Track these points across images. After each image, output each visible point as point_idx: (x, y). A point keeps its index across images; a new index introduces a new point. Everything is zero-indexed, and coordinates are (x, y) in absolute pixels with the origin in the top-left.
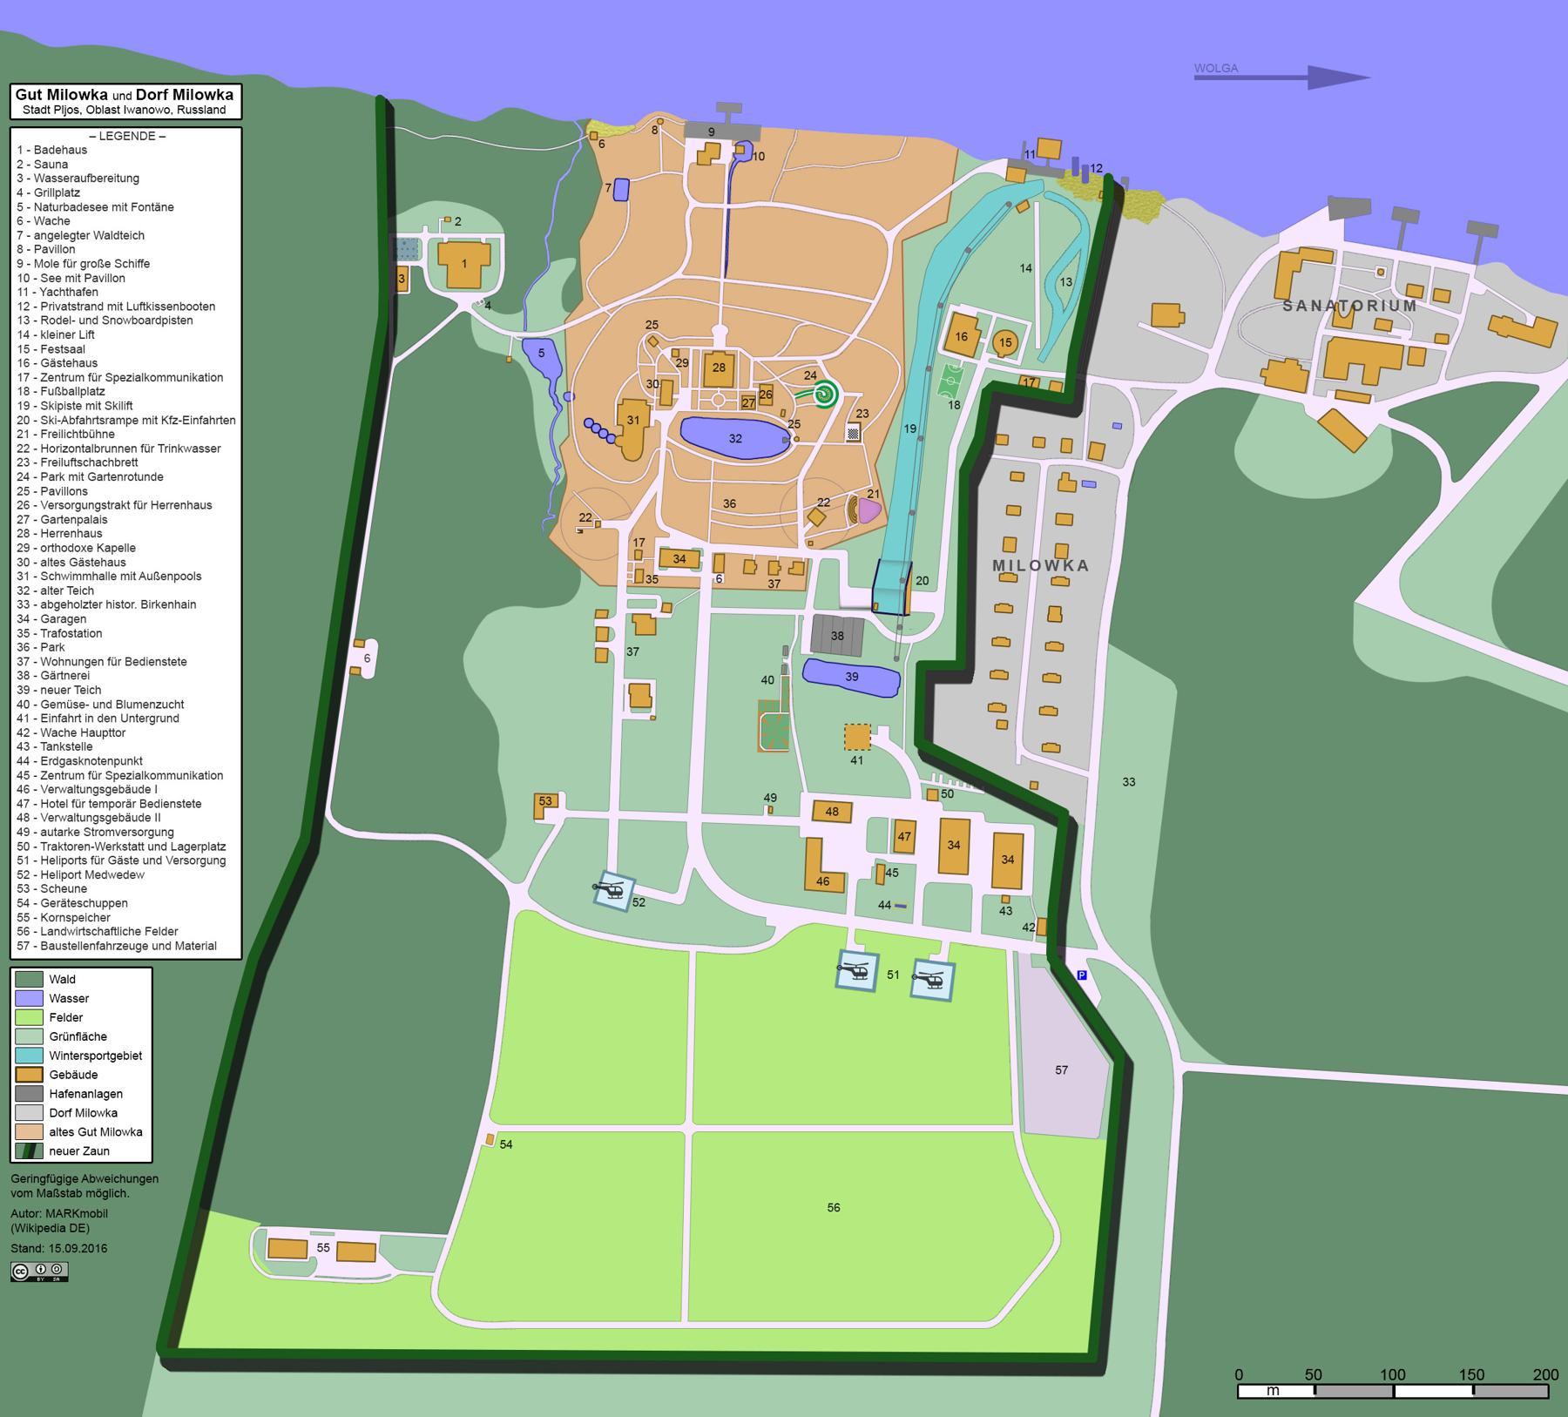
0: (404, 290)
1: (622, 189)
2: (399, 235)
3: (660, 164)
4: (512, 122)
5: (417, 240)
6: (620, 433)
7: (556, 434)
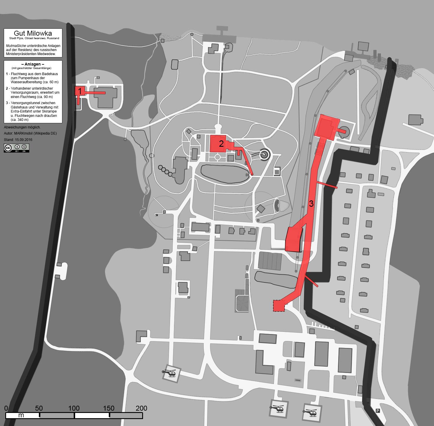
0: (79, 109)
1: (176, 65)
2: (77, 85)
3: (193, 55)
4: (127, 35)
5: (84, 87)
6: (177, 173)
7: (149, 175)
